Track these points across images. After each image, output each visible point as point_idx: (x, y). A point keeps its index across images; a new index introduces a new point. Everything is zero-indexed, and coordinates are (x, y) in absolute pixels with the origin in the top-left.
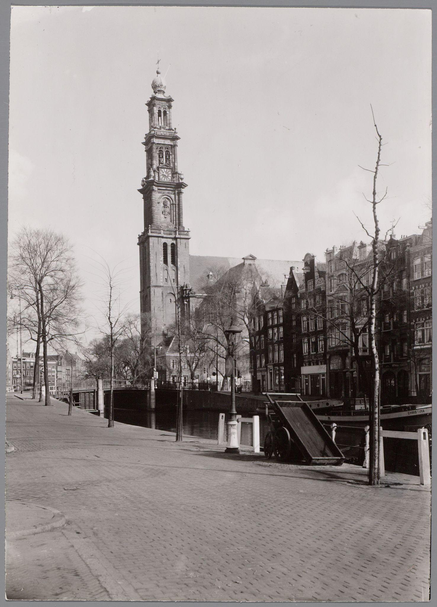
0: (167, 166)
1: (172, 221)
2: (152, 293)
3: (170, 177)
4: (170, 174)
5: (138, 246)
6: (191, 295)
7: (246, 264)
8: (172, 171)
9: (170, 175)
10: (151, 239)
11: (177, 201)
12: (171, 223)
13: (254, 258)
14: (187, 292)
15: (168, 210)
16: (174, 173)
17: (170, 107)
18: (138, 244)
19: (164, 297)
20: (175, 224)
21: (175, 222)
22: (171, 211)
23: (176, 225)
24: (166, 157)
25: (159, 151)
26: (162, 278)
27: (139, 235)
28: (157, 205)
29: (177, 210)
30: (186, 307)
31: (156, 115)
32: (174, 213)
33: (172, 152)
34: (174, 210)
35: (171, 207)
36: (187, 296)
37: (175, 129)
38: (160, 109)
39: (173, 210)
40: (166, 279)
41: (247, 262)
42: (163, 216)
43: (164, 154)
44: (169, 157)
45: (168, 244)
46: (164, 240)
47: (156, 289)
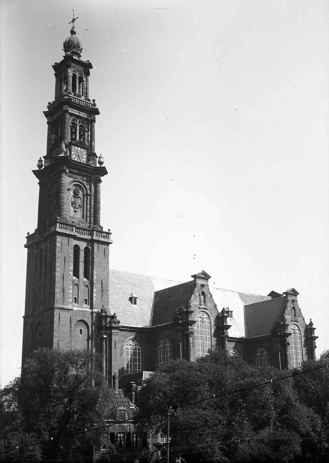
0: (81, 145)
1: (85, 218)
2: (56, 319)
3: (85, 158)
4: (84, 155)
5: (26, 249)
6: (114, 325)
7: (198, 284)
8: (87, 152)
9: (85, 156)
10: (59, 238)
11: (93, 191)
12: (83, 219)
13: (206, 277)
14: (108, 320)
15: (79, 201)
16: (91, 155)
17: (88, 74)
18: (25, 246)
19: (73, 326)
20: (88, 221)
21: (88, 218)
22: (83, 204)
23: (90, 223)
24: (80, 133)
25: (72, 123)
26: (71, 296)
27: (28, 234)
28: (66, 192)
29: (92, 203)
30: (104, 343)
31: (70, 78)
32: (88, 206)
33: (88, 128)
34: (89, 203)
35: (84, 198)
36: (108, 326)
37: (94, 101)
38: (75, 73)
39: (87, 202)
40: (75, 298)
41: (199, 282)
42: (72, 209)
43: (78, 128)
44: (84, 134)
45: (81, 248)
46: (75, 242)
47: (63, 314)
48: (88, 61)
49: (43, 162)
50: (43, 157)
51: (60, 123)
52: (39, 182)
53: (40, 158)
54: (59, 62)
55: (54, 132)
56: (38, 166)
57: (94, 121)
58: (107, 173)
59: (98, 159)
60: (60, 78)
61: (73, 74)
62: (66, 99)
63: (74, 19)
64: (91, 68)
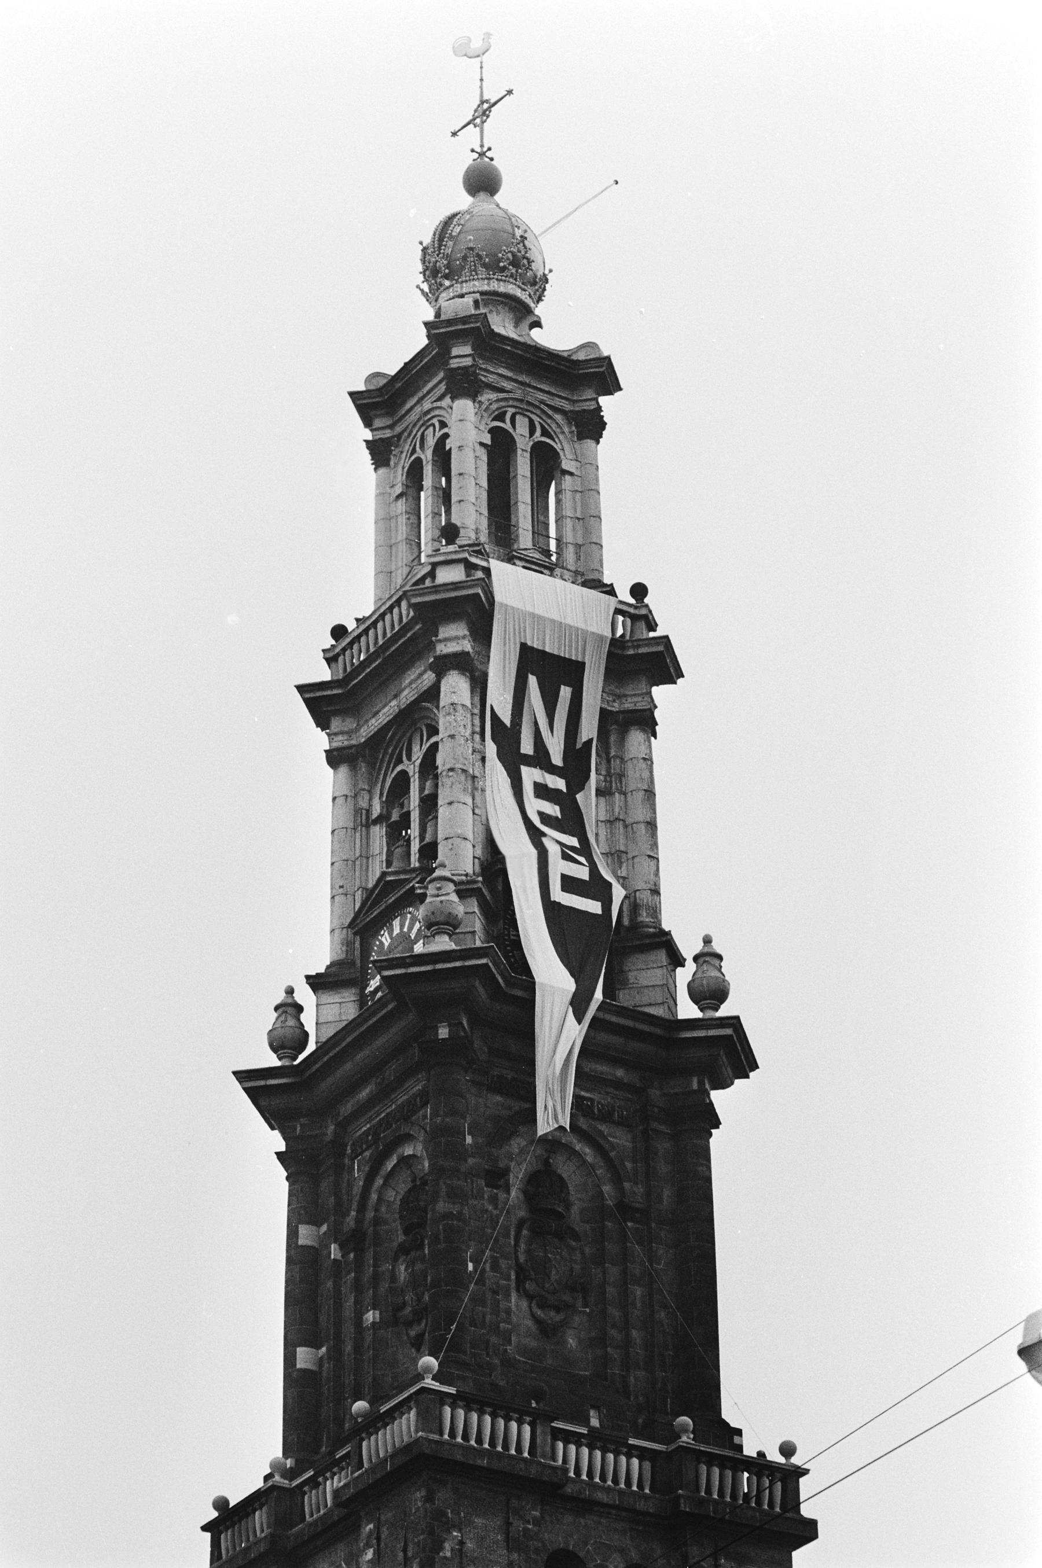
37: (639, 591)
38: (507, 426)
48: (591, 345)
49: (309, 1020)
50: (308, 977)
51: (416, 748)
52: (282, 1146)
53: (290, 991)
54: (392, 370)
55: (377, 810)
56: (277, 1045)
57: (647, 722)
58: (754, 1066)
59: (684, 975)
60: (402, 463)
61: (492, 431)
62: (455, 586)
63: (482, 102)
64: (610, 393)
